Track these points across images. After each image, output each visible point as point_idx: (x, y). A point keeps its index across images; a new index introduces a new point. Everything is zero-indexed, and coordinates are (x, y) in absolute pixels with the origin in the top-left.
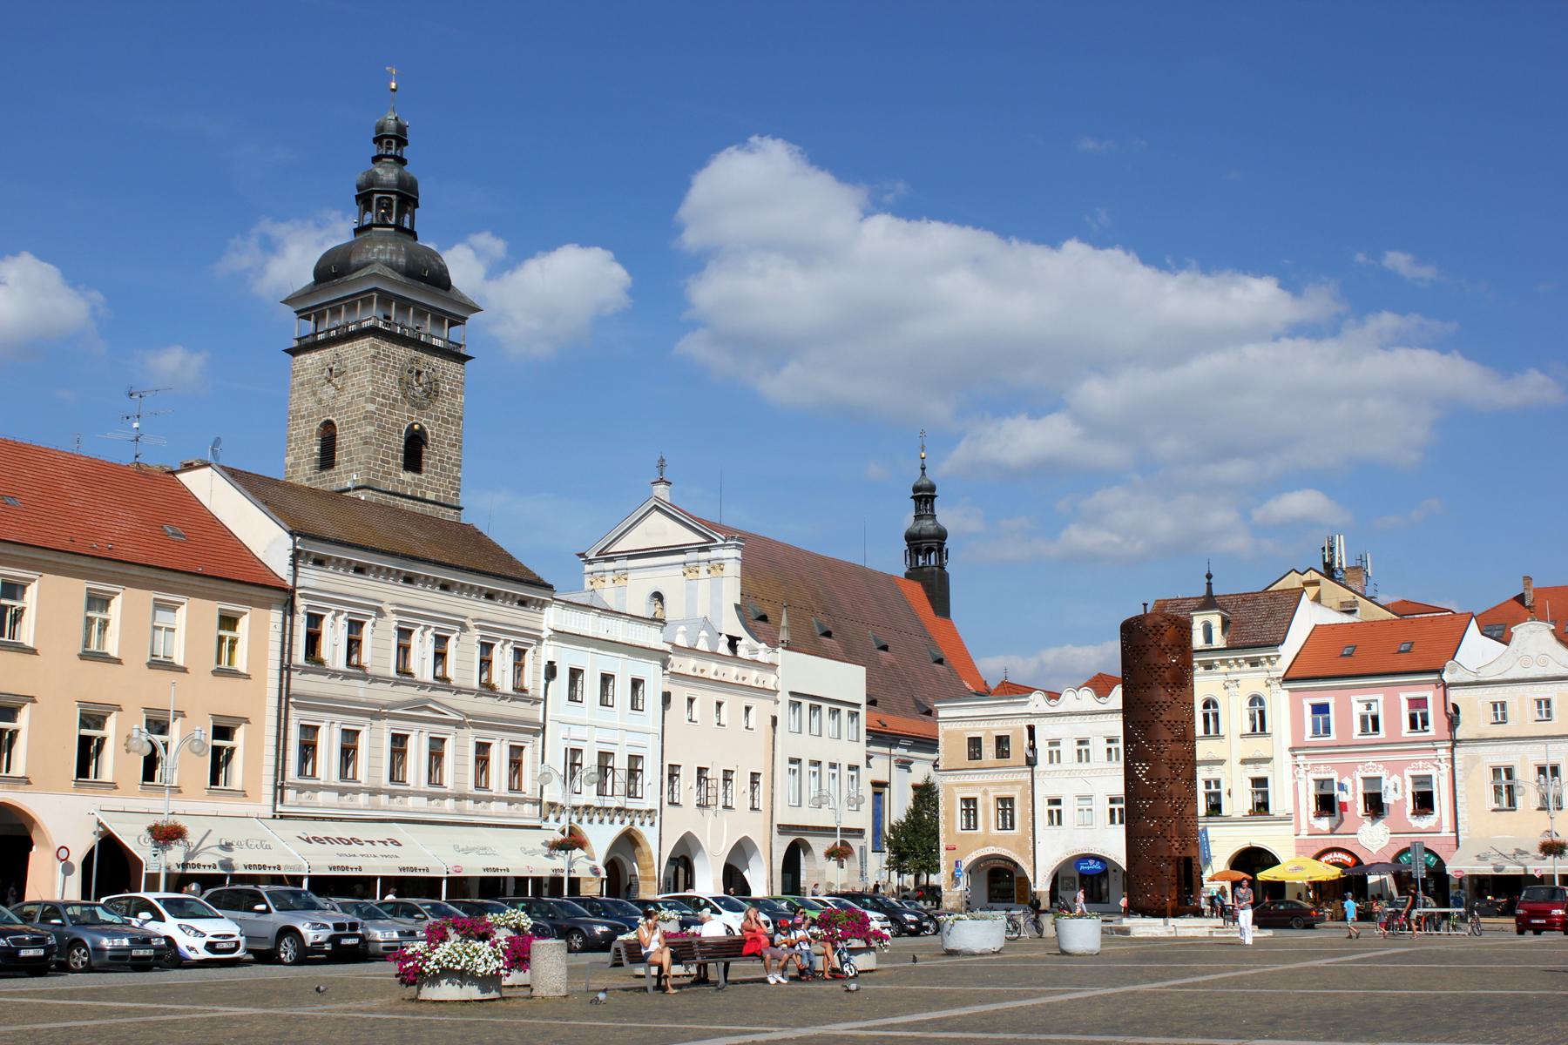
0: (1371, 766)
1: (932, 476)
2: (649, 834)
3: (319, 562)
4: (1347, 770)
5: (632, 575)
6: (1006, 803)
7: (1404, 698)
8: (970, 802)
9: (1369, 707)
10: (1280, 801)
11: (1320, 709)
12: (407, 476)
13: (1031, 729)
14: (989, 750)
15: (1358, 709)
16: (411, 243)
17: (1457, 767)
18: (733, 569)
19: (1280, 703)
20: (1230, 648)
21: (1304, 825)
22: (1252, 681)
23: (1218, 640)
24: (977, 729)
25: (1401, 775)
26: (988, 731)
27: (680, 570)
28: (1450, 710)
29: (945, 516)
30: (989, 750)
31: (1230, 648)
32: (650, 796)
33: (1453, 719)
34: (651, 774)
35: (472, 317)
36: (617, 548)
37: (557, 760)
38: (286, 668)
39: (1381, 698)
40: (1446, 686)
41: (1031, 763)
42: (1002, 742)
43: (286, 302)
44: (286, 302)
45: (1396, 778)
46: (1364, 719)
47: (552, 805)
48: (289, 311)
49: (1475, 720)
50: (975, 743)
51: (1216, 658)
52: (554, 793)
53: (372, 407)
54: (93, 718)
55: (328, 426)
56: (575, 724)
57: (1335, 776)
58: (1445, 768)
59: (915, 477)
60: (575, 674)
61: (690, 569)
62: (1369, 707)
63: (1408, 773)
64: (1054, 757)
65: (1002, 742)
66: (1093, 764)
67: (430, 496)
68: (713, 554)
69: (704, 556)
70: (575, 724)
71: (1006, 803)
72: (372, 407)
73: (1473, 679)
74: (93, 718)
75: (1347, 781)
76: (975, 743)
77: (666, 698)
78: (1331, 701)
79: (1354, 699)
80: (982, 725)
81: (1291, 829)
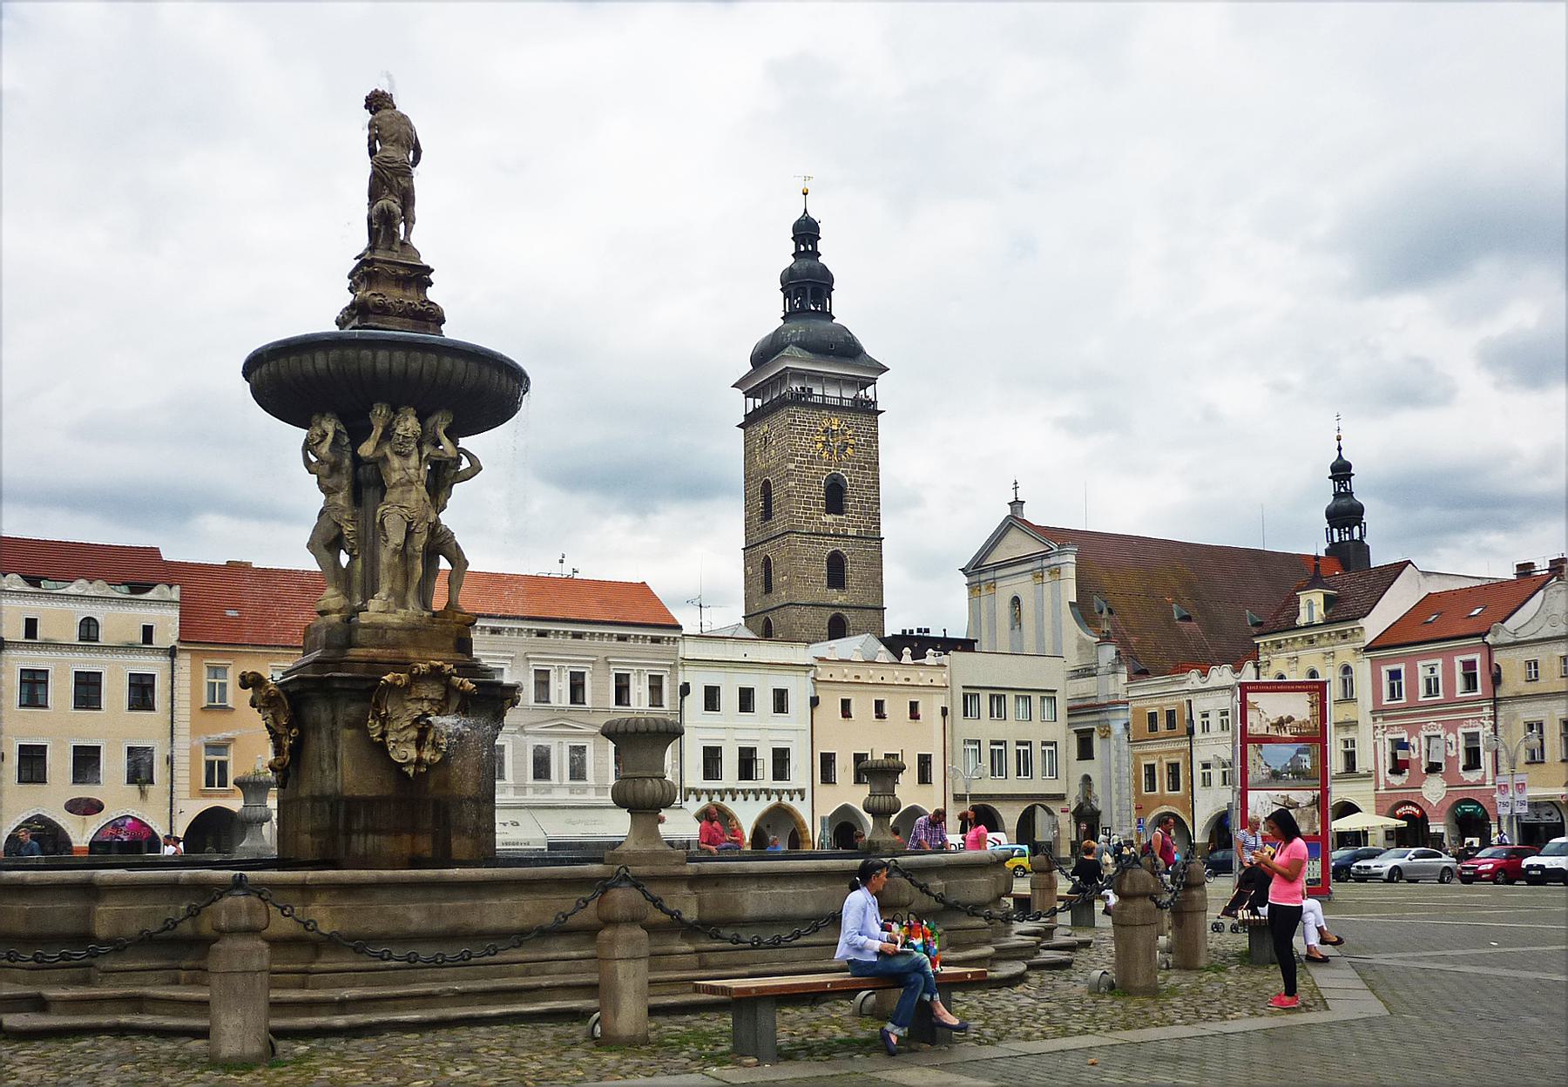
0: (1432, 725)
2: (802, 808)
4: (1414, 730)
5: (999, 584)
6: (1174, 768)
7: (1458, 660)
8: (1151, 768)
9: (1432, 670)
10: (1362, 764)
11: (1395, 675)
13: (1190, 702)
14: (1162, 724)
15: (1423, 673)
16: (822, 324)
17: (1500, 724)
18: (1070, 572)
19: (1363, 671)
20: (1328, 622)
21: (1382, 782)
22: (1345, 652)
23: (1319, 613)
24: (1153, 706)
25: (1455, 733)
26: (1161, 706)
27: (1029, 577)
28: (1494, 670)
30: (1162, 724)
31: (1328, 622)
33: (1496, 680)
35: (882, 379)
36: (992, 560)
39: (1440, 662)
40: (1490, 648)
41: (1191, 732)
42: (1170, 715)
45: (1451, 737)
46: (1429, 681)
47: (690, 790)
48: (739, 393)
49: (1514, 681)
50: (1153, 716)
51: (1313, 632)
53: (792, 466)
55: (767, 483)
57: (1405, 736)
58: (1489, 724)
61: (1038, 575)
62: (1432, 670)
63: (1461, 730)
64: (1206, 727)
65: (1170, 715)
66: (1212, 734)
67: (852, 532)
68: (1053, 561)
69: (1046, 562)
71: (1174, 768)
72: (792, 466)
73: (1512, 640)
75: (1414, 741)
76: (1153, 716)
77: (815, 702)
78: (1402, 667)
79: (1420, 664)
80: (1157, 702)
81: (1371, 786)
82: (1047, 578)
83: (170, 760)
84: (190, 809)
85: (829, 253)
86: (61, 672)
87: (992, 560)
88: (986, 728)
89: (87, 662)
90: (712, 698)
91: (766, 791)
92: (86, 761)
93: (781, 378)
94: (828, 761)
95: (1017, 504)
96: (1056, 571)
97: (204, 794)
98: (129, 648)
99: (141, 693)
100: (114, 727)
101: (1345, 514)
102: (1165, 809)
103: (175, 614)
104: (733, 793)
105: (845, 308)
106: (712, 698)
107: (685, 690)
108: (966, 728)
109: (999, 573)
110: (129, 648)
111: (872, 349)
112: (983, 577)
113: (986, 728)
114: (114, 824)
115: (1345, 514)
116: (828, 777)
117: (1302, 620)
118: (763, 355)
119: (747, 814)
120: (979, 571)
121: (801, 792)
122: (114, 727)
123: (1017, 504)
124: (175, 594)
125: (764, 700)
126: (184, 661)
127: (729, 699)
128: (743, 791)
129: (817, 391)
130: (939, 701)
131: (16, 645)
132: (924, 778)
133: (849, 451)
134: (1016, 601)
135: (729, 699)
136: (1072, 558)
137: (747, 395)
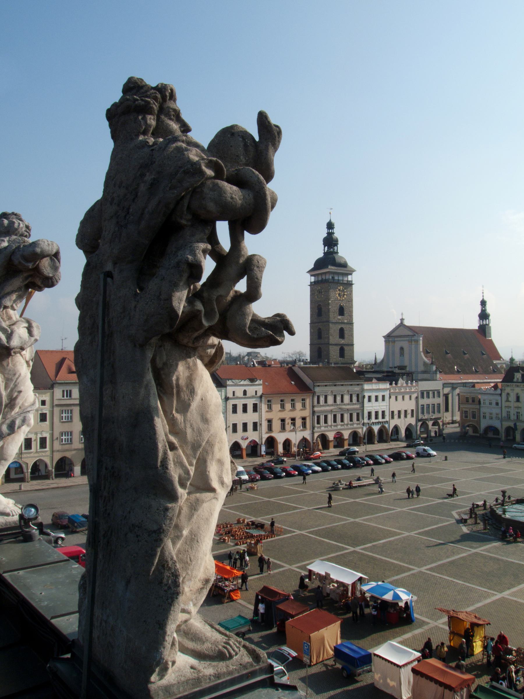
1: (485, 299)
3: (318, 386)
5: (396, 342)
12: (340, 317)
14: (470, 401)
18: (421, 342)
23: (520, 380)
27: (407, 342)
29: (489, 310)
32: (387, 418)
34: (387, 414)
35: (354, 274)
37: (366, 415)
38: (313, 407)
43: (308, 272)
44: (308, 272)
48: (308, 275)
51: (519, 384)
52: (366, 420)
54: (283, 420)
56: (369, 407)
59: (481, 299)
60: (370, 398)
61: (410, 341)
67: (346, 321)
69: (413, 338)
70: (369, 407)
74: (283, 420)
77: (390, 397)
82: (413, 343)
83: (261, 424)
84: (265, 436)
85: (337, 233)
86: (240, 404)
87: (394, 334)
88: (425, 401)
89: (244, 401)
90: (370, 400)
91: (380, 422)
92: (245, 425)
93: (325, 273)
94: (393, 412)
95: (402, 320)
96: (417, 341)
97: (267, 433)
98: (252, 397)
99: (255, 408)
100: (251, 417)
101: (484, 316)
102: (471, 423)
103: (261, 387)
104: (373, 423)
105: (343, 251)
106: (370, 400)
107: (364, 397)
108: (421, 402)
109: (396, 339)
110: (252, 397)
111: (350, 264)
112: (390, 339)
113: (425, 401)
114: (250, 442)
115: (484, 316)
116: (393, 417)
117: (515, 380)
118: (320, 264)
119: (376, 429)
120: (390, 338)
121: (387, 422)
122: (251, 417)
123: (402, 320)
124: (261, 382)
125: (380, 398)
126: (263, 399)
127: (373, 399)
128: (376, 423)
129: (336, 278)
130: (415, 395)
131: (232, 399)
132: (412, 416)
133: (345, 296)
134: (402, 349)
135: (373, 399)
136: (421, 339)
137: (311, 276)
